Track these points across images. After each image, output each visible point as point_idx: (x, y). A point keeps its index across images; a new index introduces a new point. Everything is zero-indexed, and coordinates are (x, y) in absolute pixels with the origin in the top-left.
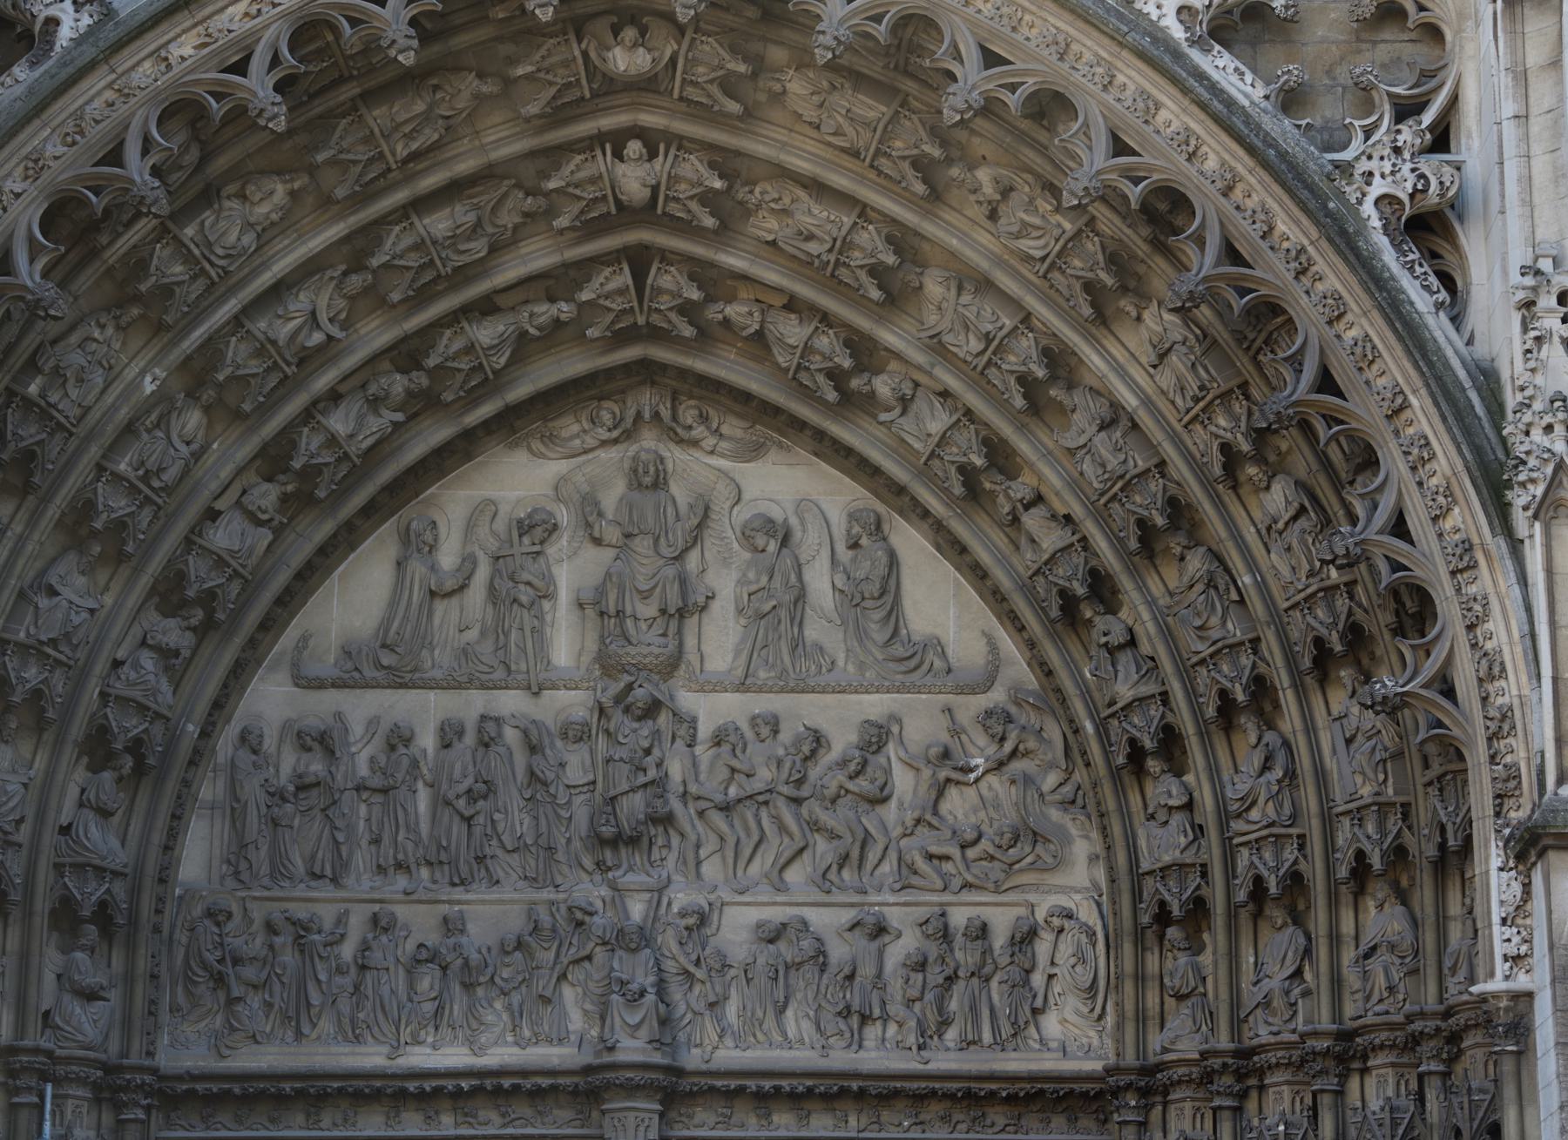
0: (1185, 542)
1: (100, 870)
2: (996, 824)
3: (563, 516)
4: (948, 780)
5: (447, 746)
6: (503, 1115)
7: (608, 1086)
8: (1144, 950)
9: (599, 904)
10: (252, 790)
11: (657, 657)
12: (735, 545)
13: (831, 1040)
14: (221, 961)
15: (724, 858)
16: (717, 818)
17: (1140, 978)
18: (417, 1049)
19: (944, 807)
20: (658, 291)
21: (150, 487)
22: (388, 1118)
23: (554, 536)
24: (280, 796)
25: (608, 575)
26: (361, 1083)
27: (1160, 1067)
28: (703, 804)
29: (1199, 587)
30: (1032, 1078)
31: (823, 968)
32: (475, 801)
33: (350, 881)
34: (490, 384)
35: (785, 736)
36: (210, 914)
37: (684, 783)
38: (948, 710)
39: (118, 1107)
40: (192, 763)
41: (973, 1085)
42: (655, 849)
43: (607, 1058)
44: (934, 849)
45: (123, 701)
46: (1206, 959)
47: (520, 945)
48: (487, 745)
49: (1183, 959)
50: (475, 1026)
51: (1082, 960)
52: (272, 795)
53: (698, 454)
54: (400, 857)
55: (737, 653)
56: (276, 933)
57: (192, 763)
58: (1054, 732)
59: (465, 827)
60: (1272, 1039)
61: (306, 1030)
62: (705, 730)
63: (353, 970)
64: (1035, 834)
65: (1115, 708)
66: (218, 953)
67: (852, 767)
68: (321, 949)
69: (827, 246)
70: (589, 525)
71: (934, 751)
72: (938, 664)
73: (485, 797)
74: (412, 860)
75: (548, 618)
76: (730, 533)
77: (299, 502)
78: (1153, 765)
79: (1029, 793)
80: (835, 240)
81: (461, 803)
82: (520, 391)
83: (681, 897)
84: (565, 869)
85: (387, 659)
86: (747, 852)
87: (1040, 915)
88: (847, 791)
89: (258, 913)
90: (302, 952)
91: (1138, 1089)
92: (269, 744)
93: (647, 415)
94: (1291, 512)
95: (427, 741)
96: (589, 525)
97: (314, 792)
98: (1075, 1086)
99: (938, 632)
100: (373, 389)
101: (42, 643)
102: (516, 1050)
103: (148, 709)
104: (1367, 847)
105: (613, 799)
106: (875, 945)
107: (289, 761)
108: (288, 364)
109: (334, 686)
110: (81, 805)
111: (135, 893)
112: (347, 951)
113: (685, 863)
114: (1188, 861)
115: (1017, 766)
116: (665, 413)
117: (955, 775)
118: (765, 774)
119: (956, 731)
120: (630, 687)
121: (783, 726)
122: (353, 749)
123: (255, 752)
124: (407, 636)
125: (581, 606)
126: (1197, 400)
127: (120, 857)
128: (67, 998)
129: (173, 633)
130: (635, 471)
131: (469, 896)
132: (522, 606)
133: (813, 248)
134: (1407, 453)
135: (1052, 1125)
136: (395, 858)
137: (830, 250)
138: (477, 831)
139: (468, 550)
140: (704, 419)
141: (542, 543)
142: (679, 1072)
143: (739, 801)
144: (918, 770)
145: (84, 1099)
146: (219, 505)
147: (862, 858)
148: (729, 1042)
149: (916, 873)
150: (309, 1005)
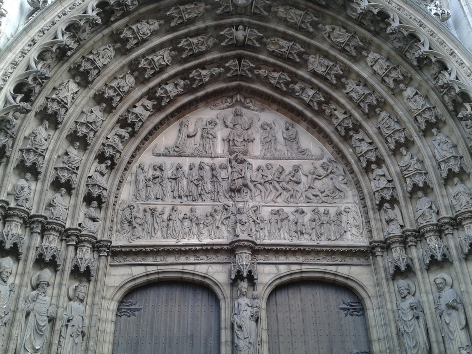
1: (99, 187)
2: (328, 189)
3: (219, 122)
4: (316, 178)
6: (207, 257)
9: (231, 205)
10: (141, 177)
12: (259, 129)
14: (131, 218)
15: (261, 196)
17: (376, 220)
18: (184, 240)
19: (315, 184)
20: (244, 66)
21: (120, 91)
24: (148, 180)
25: (231, 131)
26: (169, 248)
27: (386, 240)
28: (256, 183)
29: (387, 118)
30: (348, 247)
32: (199, 181)
33: (166, 200)
34: (202, 86)
36: (129, 206)
39: (99, 252)
42: (244, 193)
43: (237, 239)
44: (314, 193)
45: (109, 146)
48: (201, 169)
49: (390, 211)
50: (199, 234)
52: (146, 180)
53: (249, 110)
54: (179, 194)
55: (261, 151)
56: (146, 212)
57: (126, 169)
58: (341, 167)
59: (196, 188)
60: (428, 223)
61: (153, 235)
63: (166, 221)
64: (338, 190)
66: (130, 216)
67: (292, 174)
68: (158, 215)
69: (286, 49)
70: (225, 122)
71: (312, 171)
72: (310, 154)
73: (201, 180)
74: (182, 195)
76: (258, 126)
77: (158, 108)
80: (289, 47)
82: (210, 89)
83: (251, 204)
84: (222, 197)
85: (176, 149)
86: (267, 194)
88: (291, 180)
89: (142, 208)
90: (153, 216)
91: (381, 246)
92: (146, 168)
93: (239, 99)
94: (413, 94)
95: (186, 168)
96: (225, 122)
97: (157, 179)
100: (176, 82)
101: (88, 122)
102: (210, 240)
104: (452, 167)
105: (234, 180)
106: (301, 215)
107: (151, 174)
109: (163, 156)
110: (96, 171)
112: (165, 217)
113: (252, 196)
114: (388, 186)
115: (331, 176)
116: (243, 100)
118: (270, 177)
119: (315, 168)
123: (142, 169)
124: (182, 144)
126: (386, 70)
128: (87, 219)
129: (123, 132)
130: (236, 112)
131: (197, 204)
132: (209, 139)
133: (283, 50)
134: (457, 62)
137: (287, 50)
138: (199, 188)
140: (252, 102)
141: (214, 126)
143: (265, 182)
144: (307, 176)
145: (89, 247)
146: (136, 105)
147: (296, 196)
148: (267, 238)
149: (310, 199)
150: (154, 228)
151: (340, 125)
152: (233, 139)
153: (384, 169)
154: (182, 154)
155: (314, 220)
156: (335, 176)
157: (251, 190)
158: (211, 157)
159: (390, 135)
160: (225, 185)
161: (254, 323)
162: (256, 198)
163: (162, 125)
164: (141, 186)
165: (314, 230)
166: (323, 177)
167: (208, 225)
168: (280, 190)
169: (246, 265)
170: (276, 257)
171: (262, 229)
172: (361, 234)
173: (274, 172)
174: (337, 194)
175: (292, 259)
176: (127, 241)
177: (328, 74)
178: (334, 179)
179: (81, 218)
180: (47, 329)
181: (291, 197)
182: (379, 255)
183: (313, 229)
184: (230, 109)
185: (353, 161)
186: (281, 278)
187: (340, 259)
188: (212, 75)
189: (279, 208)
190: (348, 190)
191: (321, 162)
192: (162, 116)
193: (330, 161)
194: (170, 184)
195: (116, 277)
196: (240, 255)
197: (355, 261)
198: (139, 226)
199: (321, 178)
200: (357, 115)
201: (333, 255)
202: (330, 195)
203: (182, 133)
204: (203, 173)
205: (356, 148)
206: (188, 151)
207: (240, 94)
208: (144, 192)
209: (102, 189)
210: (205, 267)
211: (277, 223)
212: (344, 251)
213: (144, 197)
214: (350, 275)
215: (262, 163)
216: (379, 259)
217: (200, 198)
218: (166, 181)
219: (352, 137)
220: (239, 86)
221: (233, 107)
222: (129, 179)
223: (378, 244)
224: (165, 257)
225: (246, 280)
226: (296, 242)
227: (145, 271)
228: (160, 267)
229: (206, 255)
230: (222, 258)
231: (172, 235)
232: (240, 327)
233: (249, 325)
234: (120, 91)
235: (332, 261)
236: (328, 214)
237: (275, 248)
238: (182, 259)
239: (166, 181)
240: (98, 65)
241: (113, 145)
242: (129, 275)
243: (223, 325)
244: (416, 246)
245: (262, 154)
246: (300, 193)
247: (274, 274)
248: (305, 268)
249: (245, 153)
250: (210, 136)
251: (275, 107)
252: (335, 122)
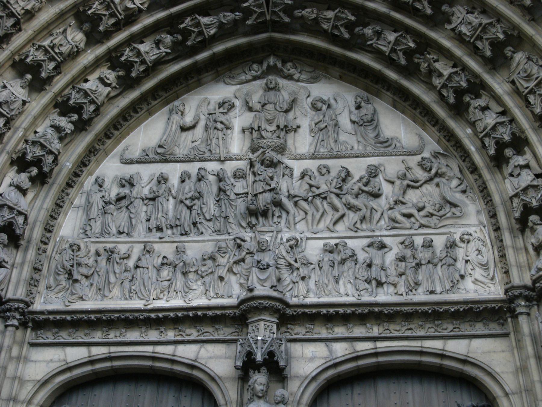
0: (512, 49)
2: (431, 203)
3: (237, 103)
5: (183, 181)
6: (198, 331)
8: (514, 237)
9: (248, 239)
10: (96, 199)
11: (276, 143)
12: (309, 110)
13: (362, 293)
15: (307, 222)
16: (303, 204)
17: (516, 249)
18: (158, 301)
21: (56, 53)
22: (142, 333)
23: (233, 109)
26: (128, 315)
30: (465, 302)
31: (356, 263)
33: (135, 234)
37: (288, 191)
40: (69, 185)
41: (435, 307)
44: (405, 211)
50: (187, 290)
55: (311, 144)
56: (99, 255)
58: (454, 164)
59: (188, 212)
61: (106, 293)
63: (133, 270)
65: (487, 130)
66: (71, 262)
67: (364, 180)
68: (118, 260)
72: (398, 145)
73: (198, 199)
74: (164, 225)
75: (230, 136)
78: (508, 152)
79: (446, 187)
82: (219, 48)
83: (286, 235)
84: (233, 226)
85: (160, 150)
86: (318, 216)
87: (457, 237)
88: (363, 191)
89: (93, 249)
92: (106, 185)
93: (272, 64)
95: (174, 181)
96: (247, 103)
97: (124, 201)
98: (488, 305)
99: (397, 135)
103: (46, 147)
105: (256, 195)
106: (380, 252)
107: (114, 192)
108: (121, 14)
110: (11, 185)
112: (131, 263)
113: (289, 224)
116: (279, 65)
118: (324, 188)
120: (264, 153)
121: (331, 171)
122: (143, 185)
123: (101, 186)
129: (63, 122)
132: (218, 130)
135: (477, 327)
136: (156, 224)
138: (194, 212)
139: (198, 113)
142: (288, 305)
143: (314, 197)
148: (311, 295)
150: (109, 283)
151: (447, 86)
152: (259, 127)
153: (528, 156)
154: (168, 157)
156: (444, 180)
157: (288, 213)
159: (532, 89)
160: (241, 205)
162: (298, 226)
163: (137, 112)
164: (94, 212)
165: (403, 277)
166: (421, 182)
167: (204, 274)
168: (342, 209)
169: (264, 341)
170: (327, 328)
172: (492, 279)
173: (331, 178)
174: (448, 210)
175: (359, 331)
176: (62, 303)
178: (441, 185)
181: (361, 223)
182: (521, 313)
183: (401, 275)
184: (258, 82)
185: (472, 149)
186: (336, 365)
187: (451, 327)
188: (221, 25)
189: (337, 241)
190: (468, 202)
191: (418, 158)
192: (134, 95)
193: (436, 155)
194: (145, 208)
195: (38, 364)
196: (256, 324)
197: (479, 328)
198: (85, 279)
199: (418, 184)
200: (473, 64)
201: (437, 320)
202: (435, 213)
203: (171, 123)
204: (203, 186)
205: (477, 123)
206: (181, 152)
207: (274, 55)
208: (99, 223)
209: (15, 212)
210: (194, 348)
211: (333, 267)
212: (457, 312)
214: (469, 355)
215: (312, 165)
216: (523, 320)
217: (194, 230)
218: (138, 203)
219: (468, 104)
220: (271, 40)
221: (263, 78)
223: (519, 291)
224: (123, 330)
225: (264, 370)
226: (366, 298)
227: (87, 355)
228: (113, 349)
229: (195, 327)
230: (225, 332)
231: (140, 295)
234: (56, 53)
235: (436, 331)
236: (430, 246)
237: (324, 311)
238: (153, 335)
239: (138, 203)
240: (14, 11)
241: (42, 141)
242: (59, 361)
245: (312, 151)
246: (379, 214)
247: (322, 358)
248: (382, 345)
249: (281, 149)
250: (219, 126)
251: (336, 71)
252: (438, 82)
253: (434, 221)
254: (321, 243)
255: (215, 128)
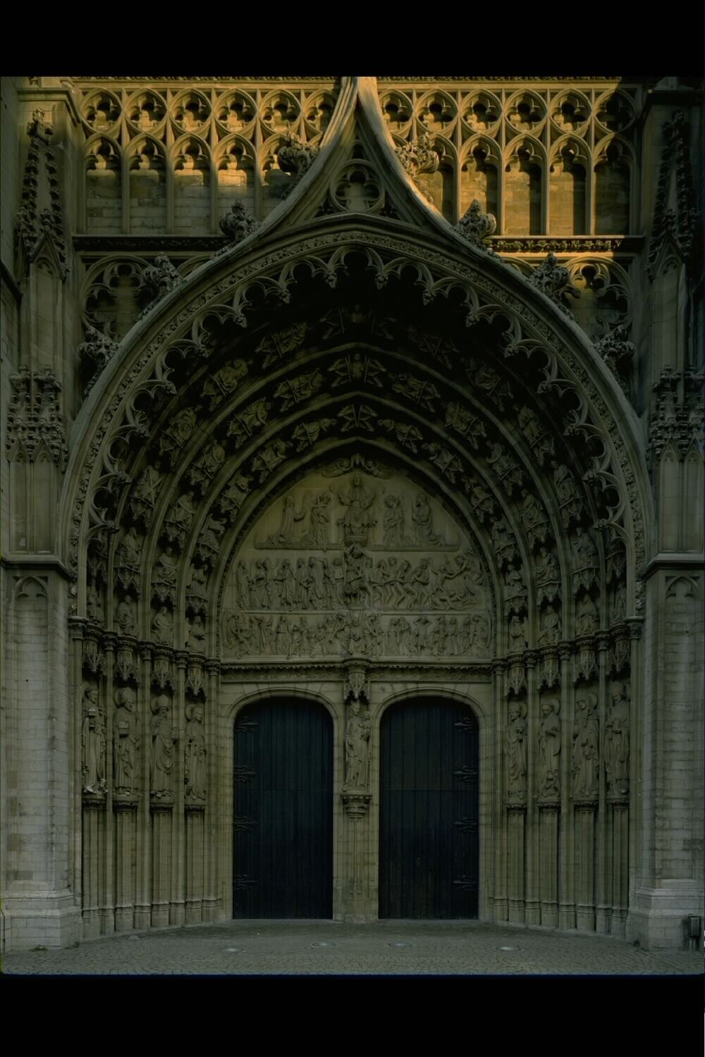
4: (446, 577)
5: (300, 567)
7: (351, 665)
16: (379, 589)
17: (503, 633)
27: (509, 658)
35: (399, 564)
36: (233, 617)
38: (445, 556)
40: (226, 570)
44: (443, 598)
46: (525, 625)
47: (324, 627)
48: (311, 566)
51: (483, 630)
58: (477, 561)
61: (262, 649)
62: (375, 563)
67: (418, 573)
71: (443, 568)
72: (443, 542)
81: (305, 584)
83: (369, 613)
85: (282, 539)
86: (388, 598)
92: (247, 567)
97: (262, 581)
107: (254, 573)
111: (210, 607)
117: (448, 576)
119: (448, 563)
125: (338, 524)
127: (206, 596)
128: (193, 638)
138: (310, 592)
144: (437, 574)
155: (438, 632)
157: (369, 594)
158: (323, 549)
161: (364, 743)
164: (244, 589)
168: (404, 594)
171: (379, 644)
175: (409, 677)
177: (469, 434)
179: (186, 637)
180: (173, 751)
183: (435, 642)
189: (398, 617)
197: (476, 678)
213: (248, 604)
215: (385, 556)
222: (230, 581)
225: (358, 701)
230: (333, 677)
232: (351, 746)
233: (360, 744)
237: (391, 666)
243: (335, 742)
244: (533, 668)
248: (421, 686)
249: (364, 544)
253: (460, 604)
254: (389, 618)
255: (319, 522)
